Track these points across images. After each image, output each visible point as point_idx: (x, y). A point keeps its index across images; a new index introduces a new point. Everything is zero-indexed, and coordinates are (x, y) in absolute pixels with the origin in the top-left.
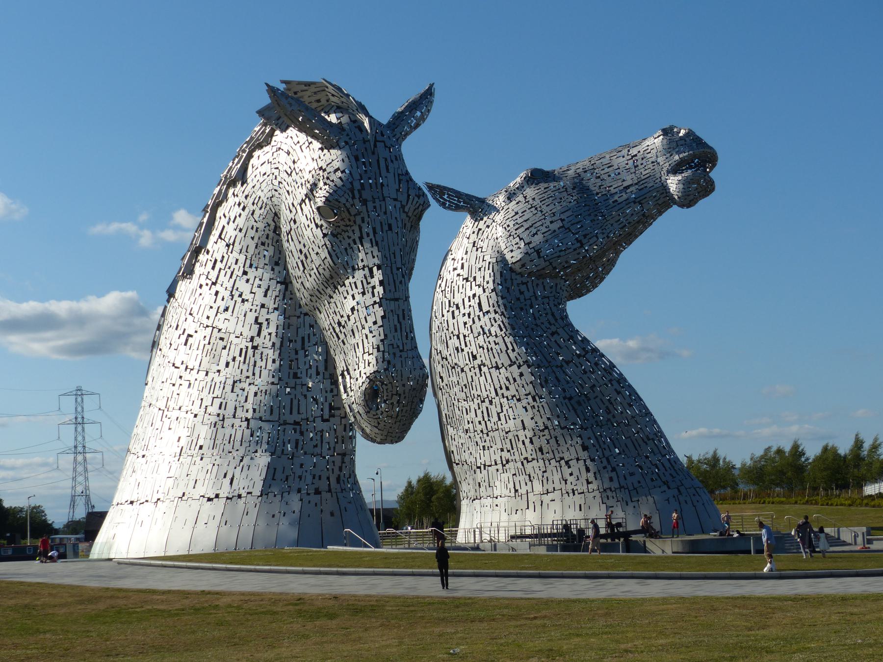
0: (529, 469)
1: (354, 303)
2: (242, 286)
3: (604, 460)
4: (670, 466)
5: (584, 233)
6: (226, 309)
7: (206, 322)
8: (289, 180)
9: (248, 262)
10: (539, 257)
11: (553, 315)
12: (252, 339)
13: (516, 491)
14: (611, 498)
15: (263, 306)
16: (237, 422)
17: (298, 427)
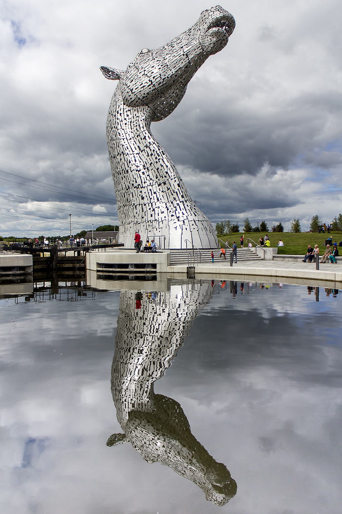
4: (183, 207)
5: (153, 76)
10: (132, 93)
11: (139, 125)
13: (122, 222)
14: (150, 226)
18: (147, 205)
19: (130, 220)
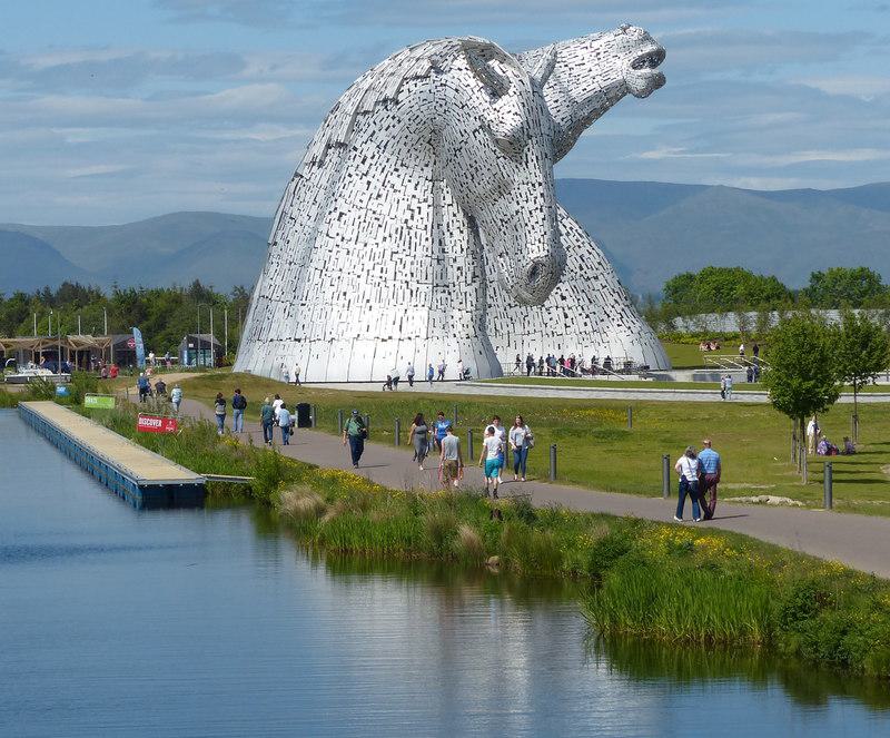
0: (511, 312)
1: (518, 207)
2: (393, 179)
3: (579, 308)
6: (379, 196)
7: (359, 205)
8: (461, 112)
9: (399, 162)
12: (406, 221)
15: (414, 196)
16: (398, 284)
17: (446, 289)
18: (574, 308)
19: (531, 329)
